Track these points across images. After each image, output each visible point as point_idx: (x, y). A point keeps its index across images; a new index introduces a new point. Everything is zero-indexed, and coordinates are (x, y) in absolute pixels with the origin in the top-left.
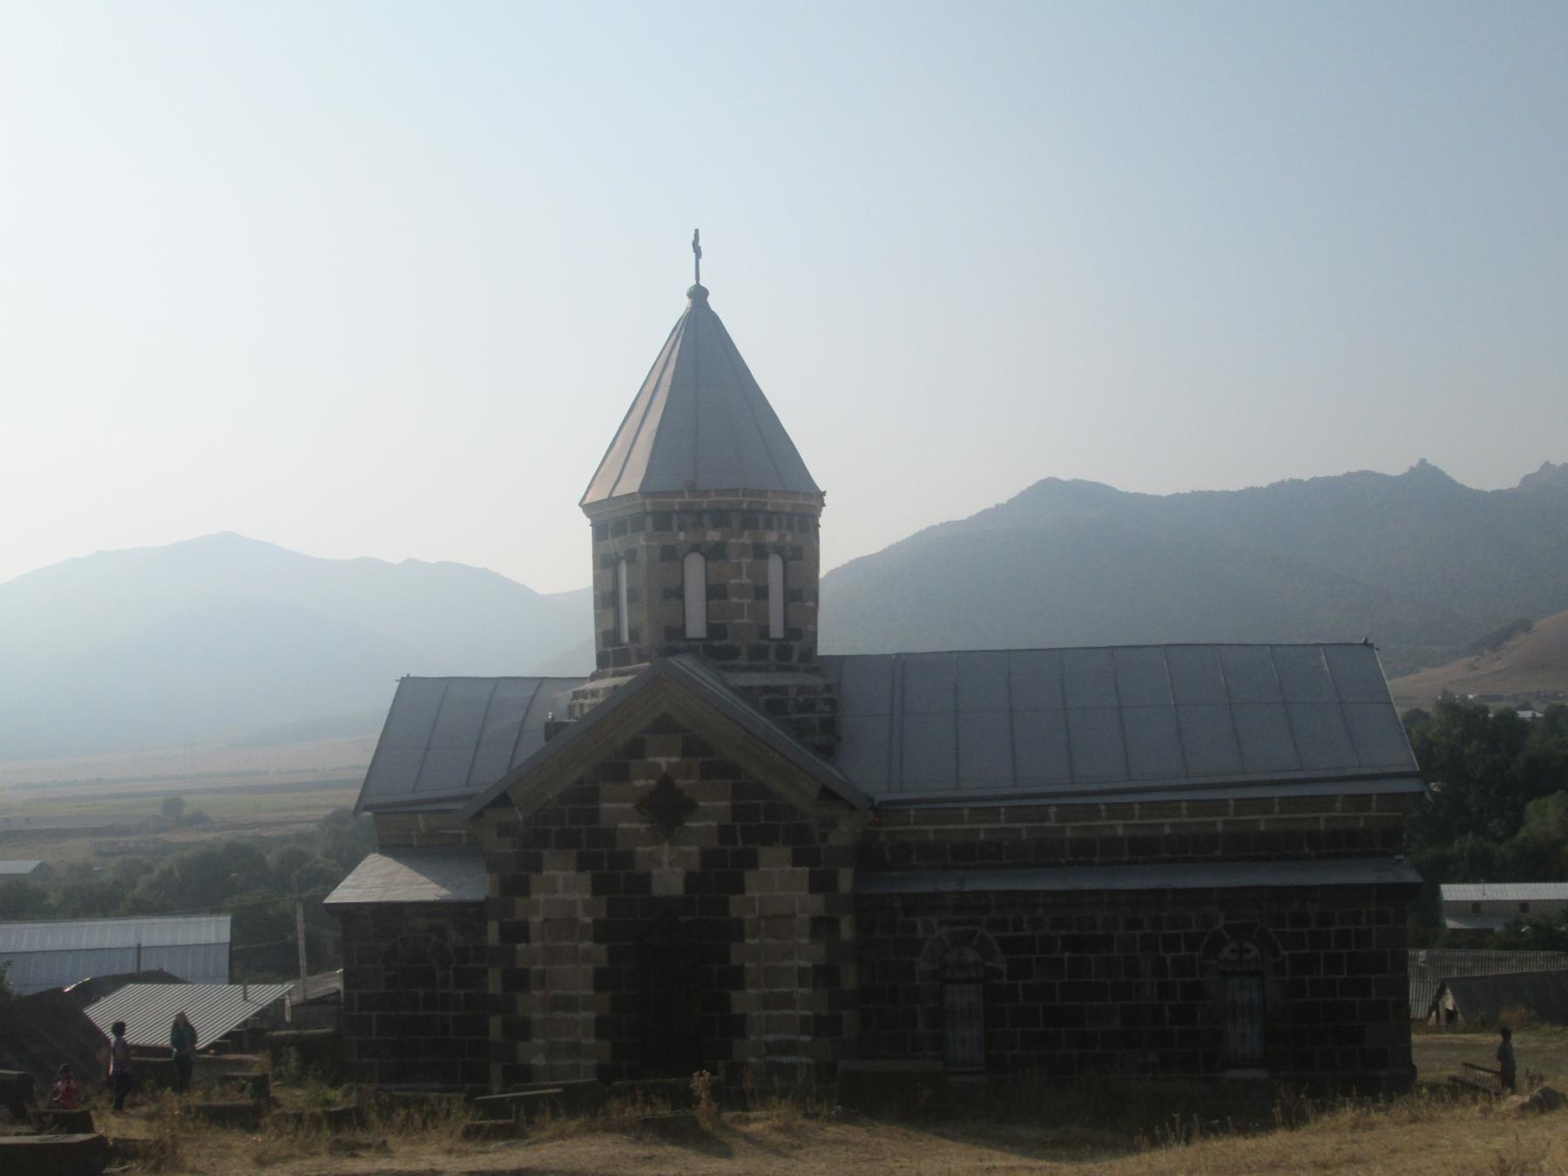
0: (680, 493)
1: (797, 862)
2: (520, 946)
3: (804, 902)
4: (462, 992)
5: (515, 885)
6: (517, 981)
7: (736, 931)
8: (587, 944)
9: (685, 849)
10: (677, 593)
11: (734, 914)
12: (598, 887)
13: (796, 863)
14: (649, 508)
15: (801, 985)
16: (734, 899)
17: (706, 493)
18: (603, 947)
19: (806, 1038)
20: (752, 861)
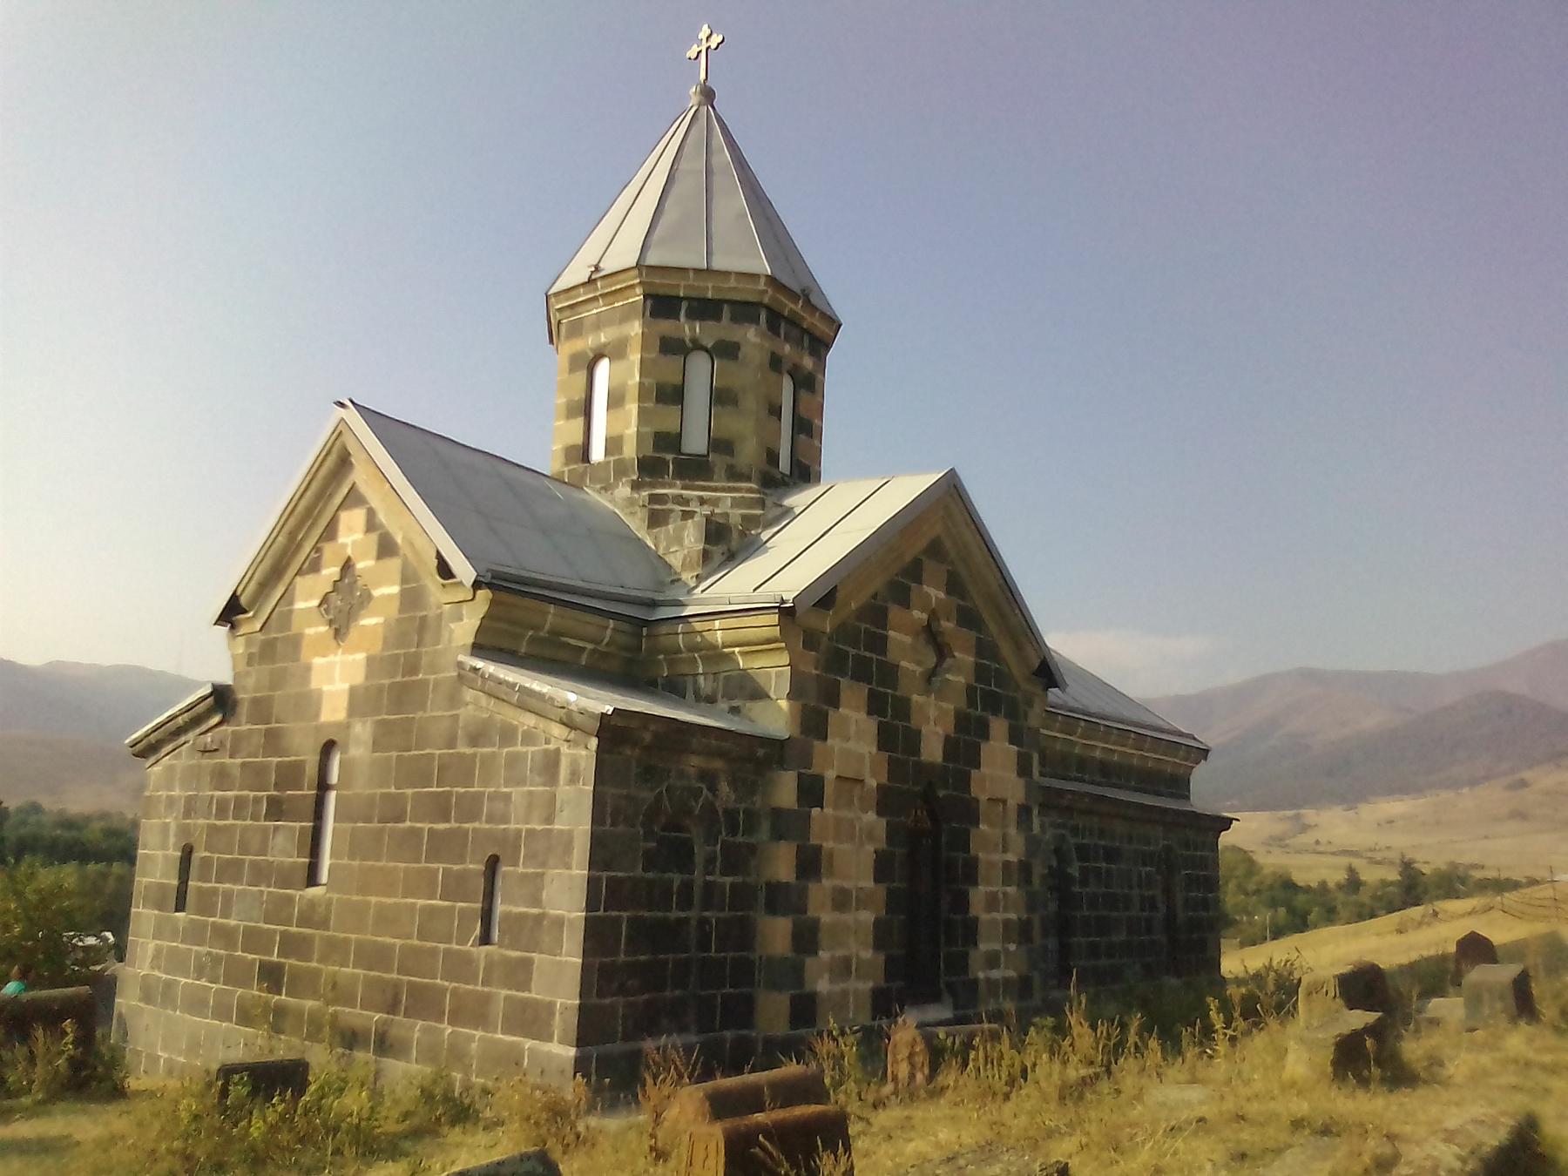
0: (794, 296)
1: (1015, 737)
2: (815, 811)
3: (1014, 790)
4: (729, 880)
5: (814, 723)
6: (810, 864)
7: (969, 813)
8: (871, 816)
9: (944, 705)
10: (776, 411)
11: (975, 791)
12: (886, 739)
13: (1011, 742)
14: (766, 300)
15: (1006, 883)
16: (974, 772)
17: (814, 308)
18: (883, 821)
19: (1012, 947)
20: (984, 733)
